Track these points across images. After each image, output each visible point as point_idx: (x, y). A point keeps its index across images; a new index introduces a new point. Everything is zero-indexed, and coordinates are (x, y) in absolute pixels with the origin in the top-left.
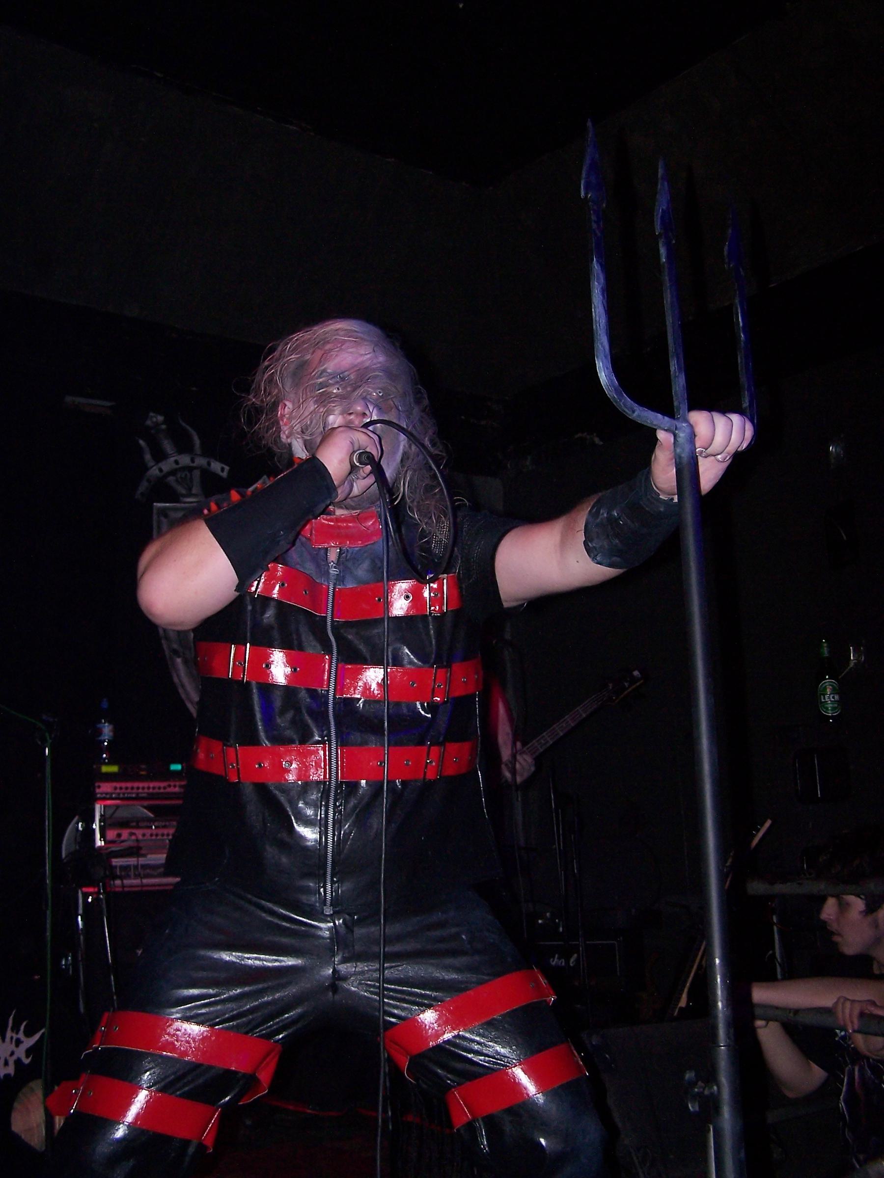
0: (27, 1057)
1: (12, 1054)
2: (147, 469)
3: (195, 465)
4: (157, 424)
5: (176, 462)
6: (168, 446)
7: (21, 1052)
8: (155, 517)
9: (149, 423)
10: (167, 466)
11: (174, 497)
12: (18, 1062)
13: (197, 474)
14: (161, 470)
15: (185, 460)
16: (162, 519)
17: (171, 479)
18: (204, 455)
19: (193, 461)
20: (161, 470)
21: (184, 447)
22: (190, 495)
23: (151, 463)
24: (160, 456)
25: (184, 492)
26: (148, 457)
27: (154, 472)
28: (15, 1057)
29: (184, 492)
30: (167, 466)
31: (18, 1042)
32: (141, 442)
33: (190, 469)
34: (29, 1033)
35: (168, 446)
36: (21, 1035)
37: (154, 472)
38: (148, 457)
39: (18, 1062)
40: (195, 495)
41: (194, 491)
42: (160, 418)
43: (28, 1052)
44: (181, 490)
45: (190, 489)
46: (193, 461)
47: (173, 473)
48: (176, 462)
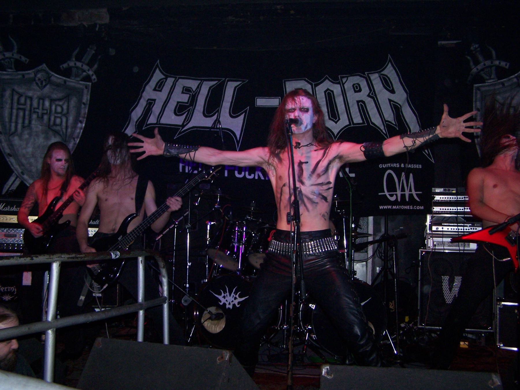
0: (238, 304)
1: (232, 301)
2: (471, 70)
3: (492, 65)
4: (476, 48)
5: (485, 65)
6: (480, 58)
7: (236, 302)
8: (474, 91)
9: (472, 48)
10: (480, 67)
11: (482, 81)
12: (234, 305)
13: (493, 68)
14: (477, 69)
15: (488, 63)
16: (478, 92)
17: (482, 72)
18: (498, 58)
19: (492, 63)
20: (477, 69)
21: (488, 56)
22: (490, 79)
23: (473, 67)
24: (477, 63)
25: (488, 78)
26: (471, 64)
27: (474, 70)
28: (233, 303)
29: (488, 78)
30: (480, 67)
31: (235, 298)
32: (469, 58)
33: (490, 67)
34: (240, 296)
35: (480, 58)
36: (237, 296)
37: (474, 70)
38: (471, 64)
39: (234, 305)
40: (493, 79)
41: (493, 76)
42: (477, 46)
43: (239, 303)
44: (486, 77)
45: (491, 76)
46: (492, 63)
47: (482, 70)
48: (485, 65)
